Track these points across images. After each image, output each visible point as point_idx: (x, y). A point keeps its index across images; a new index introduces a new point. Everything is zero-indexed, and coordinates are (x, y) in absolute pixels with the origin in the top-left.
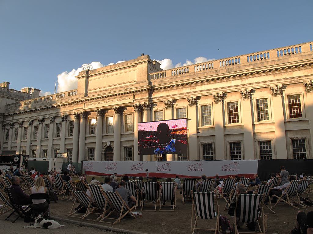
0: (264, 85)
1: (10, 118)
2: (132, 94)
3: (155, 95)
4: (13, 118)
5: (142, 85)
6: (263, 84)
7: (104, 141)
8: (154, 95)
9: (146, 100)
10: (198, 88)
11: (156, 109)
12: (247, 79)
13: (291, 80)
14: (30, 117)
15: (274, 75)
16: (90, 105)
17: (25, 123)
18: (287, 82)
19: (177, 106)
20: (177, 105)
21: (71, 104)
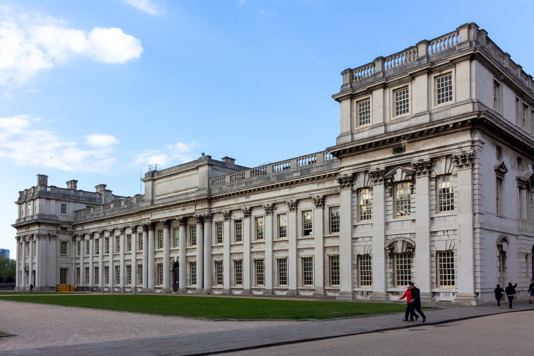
0: (309, 195)
1: (79, 229)
2: (194, 203)
4: (83, 228)
5: (202, 192)
7: (172, 255)
9: (206, 210)
10: (253, 197)
11: (217, 220)
12: (294, 188)
13: (332, 190)
14: (100, 227)
15: (318, 183)
16: (156, 214)
17: (116, 231)
18: (328, 192)
20: (235, 216)
21: (139, 213)
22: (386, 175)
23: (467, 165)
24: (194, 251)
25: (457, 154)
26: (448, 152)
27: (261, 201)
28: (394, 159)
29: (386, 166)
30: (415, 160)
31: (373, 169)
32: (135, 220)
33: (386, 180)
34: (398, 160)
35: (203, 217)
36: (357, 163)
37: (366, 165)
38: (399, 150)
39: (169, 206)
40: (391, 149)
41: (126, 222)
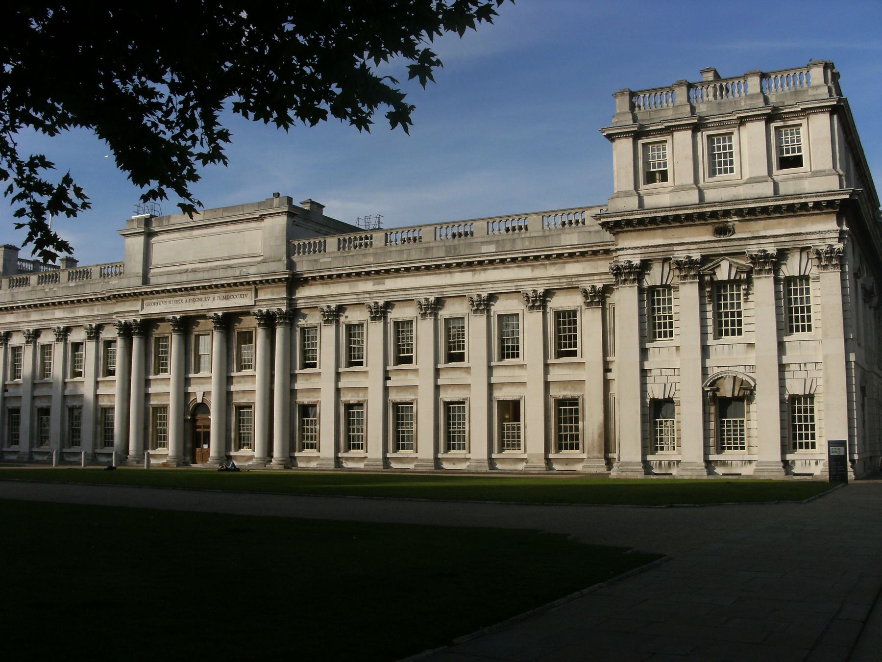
0: (514, 288)
2: (253, 286)
3: (303, 293)
5: (273, 267)
6: (510, 284)
8: (299, 292)
10: (391, 283)
12: (482, 272)
13: (561, 281)
15: (534, 267)
16: (155, 304)
19: (348, 320)
20: (347, 317)
22: (702, 268)
23: (834, 266)
24: (246, 382)
25: (820, 248)
26: (805, 242)
27: (410, 292)
28: (716, 245)
29: (703, 254)
30: (753, 249)
31: (681, 255)
32: (96, 313)
33: (701, 277)
34: (722, 247)
35: (274, 314)
36: (650, 245)
37: (666, 248)
38: (723, 231)
39: (192, 289)
40: (710, 228)
41: (72, 315)
